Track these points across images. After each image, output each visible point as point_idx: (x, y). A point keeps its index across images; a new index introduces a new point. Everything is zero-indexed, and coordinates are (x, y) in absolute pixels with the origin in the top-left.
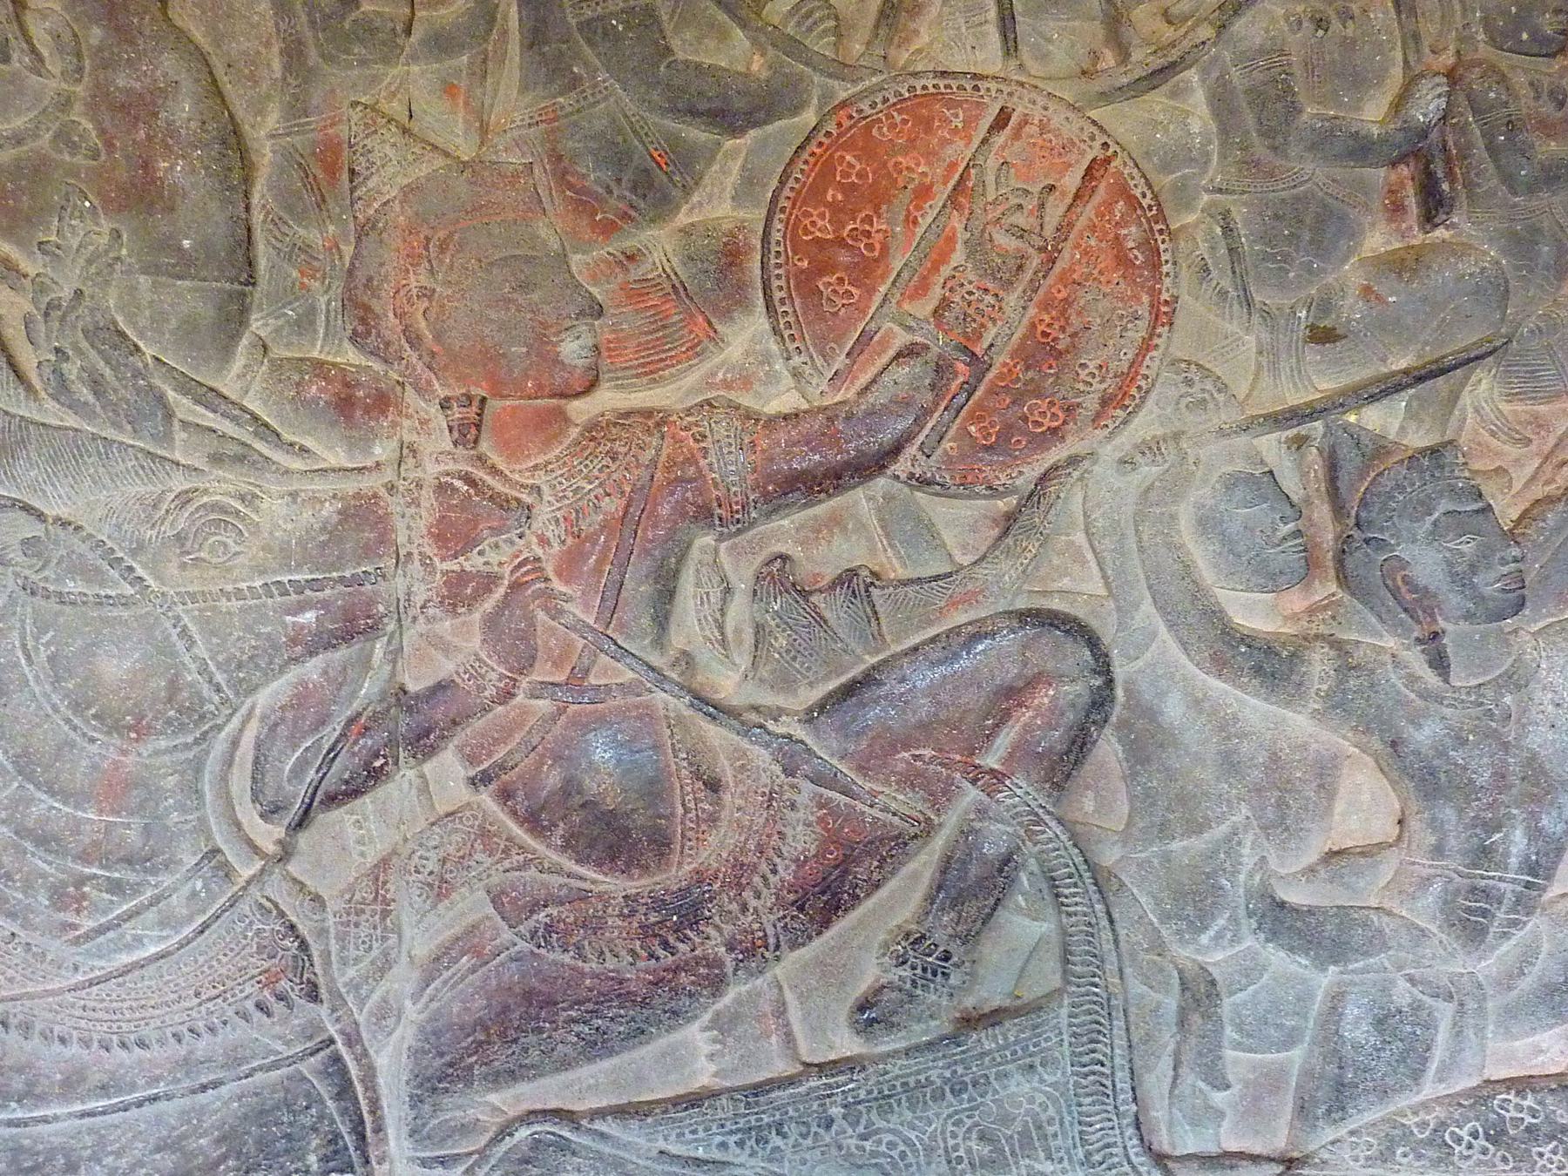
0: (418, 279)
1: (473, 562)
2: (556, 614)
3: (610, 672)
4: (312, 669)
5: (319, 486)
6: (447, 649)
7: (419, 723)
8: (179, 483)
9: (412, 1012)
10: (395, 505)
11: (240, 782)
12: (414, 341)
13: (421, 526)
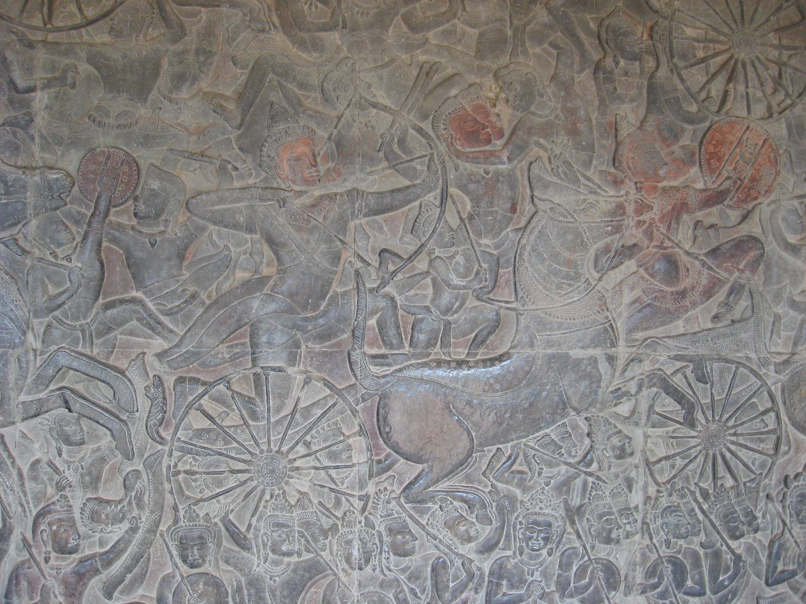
0: (631, 155)
1: (641, 218)
2: (658, 230)
3: (667, 243)
4: (609, 239)
5: (610, 199)
6: (635, 237)
7: (630, 251)
8: (582, 197)
9: (625, 314)
10: (626, 204)
11: (591, 265)
12: (630, 169)
13: (632, 209)
